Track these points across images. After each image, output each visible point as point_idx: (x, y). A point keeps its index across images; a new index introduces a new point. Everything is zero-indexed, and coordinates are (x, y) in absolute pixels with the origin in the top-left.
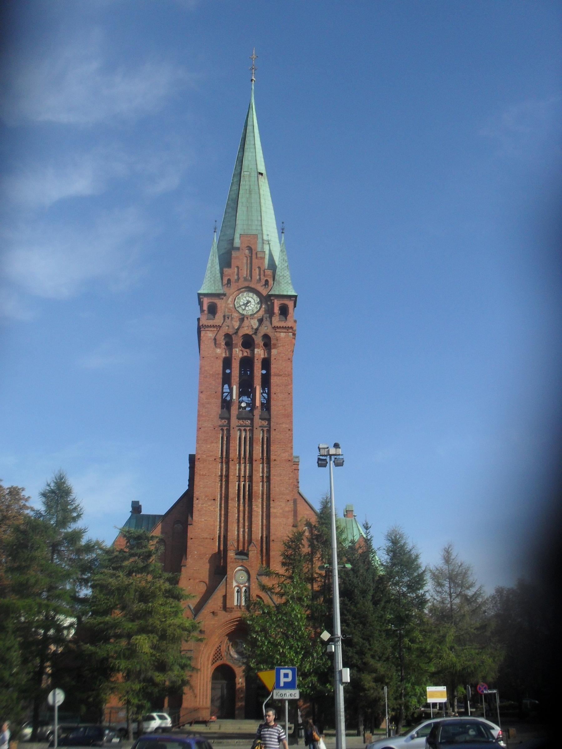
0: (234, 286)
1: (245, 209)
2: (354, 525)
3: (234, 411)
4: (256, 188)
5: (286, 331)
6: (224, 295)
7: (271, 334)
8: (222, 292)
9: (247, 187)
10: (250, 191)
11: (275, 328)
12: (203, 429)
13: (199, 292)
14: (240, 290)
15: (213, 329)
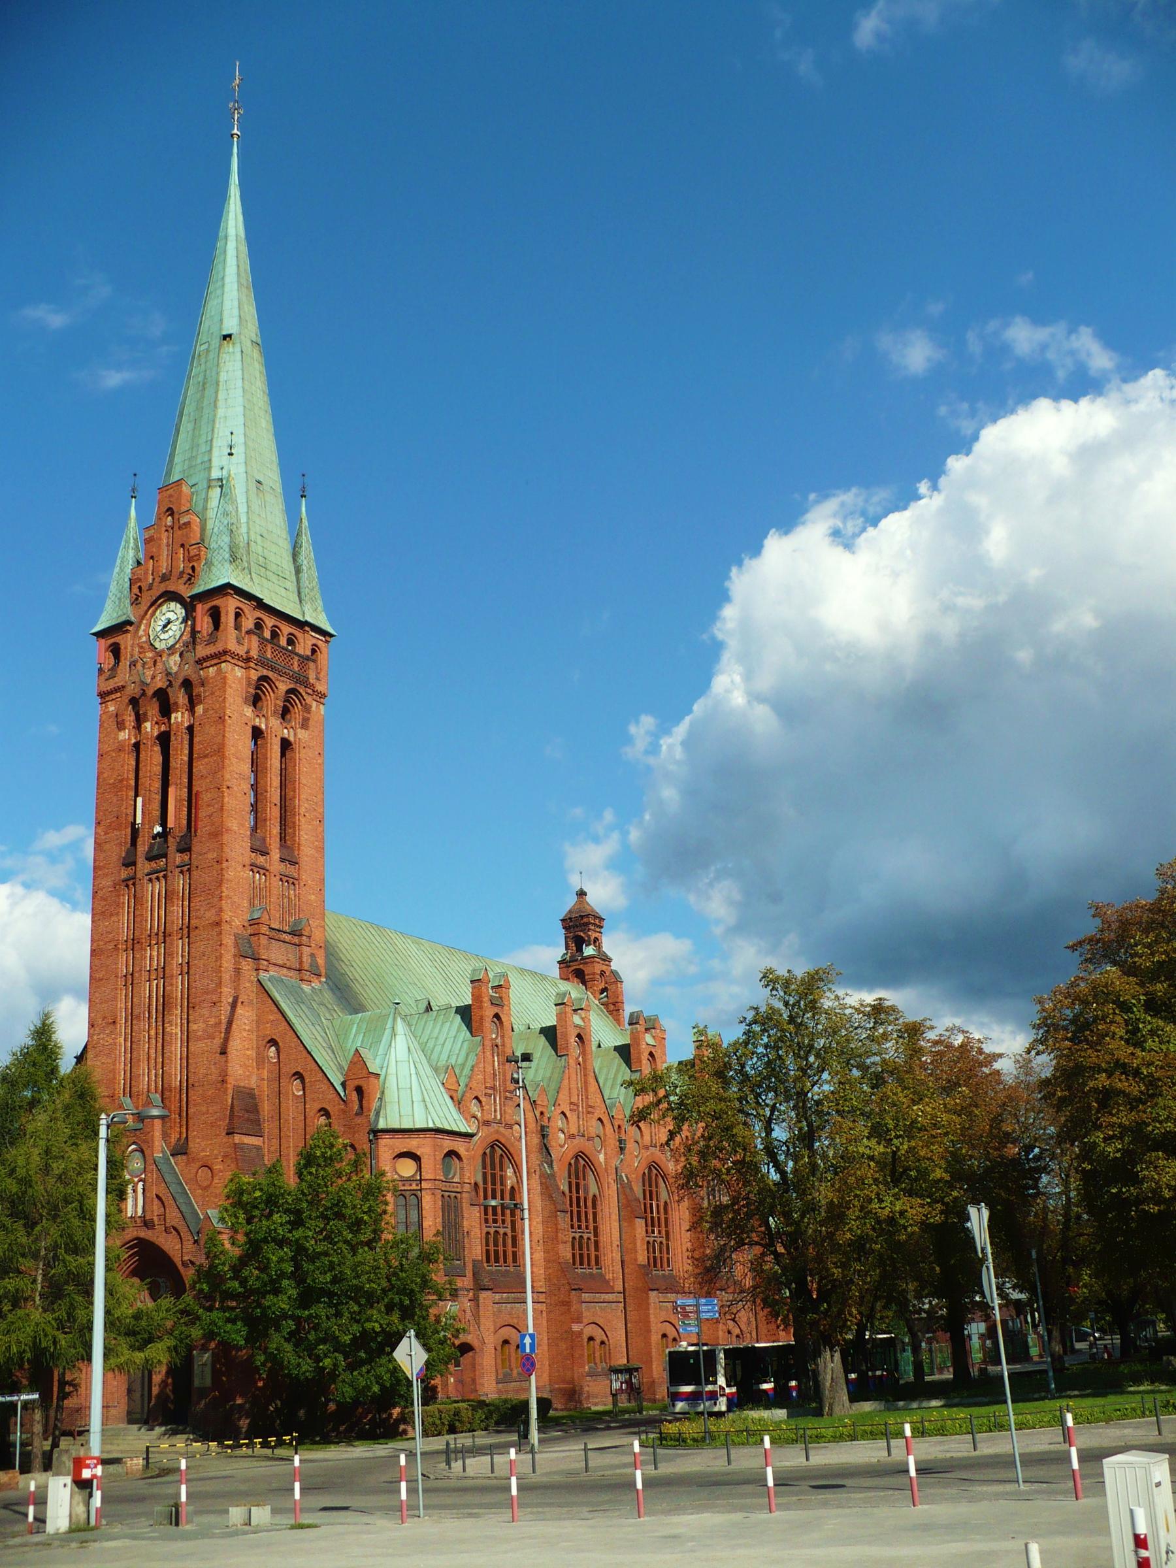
0: (146, 599)
1: (190, 426)
2: (389, 1025)
3: (142, 849)
4: (214, 373)
5: (216, 661)
6: (129, 623)
7: (194, 678)
8: (123, 618)
9: (200, 379)
10: (204, 384)
11: (200, 662)
12: (100, 894)
13: (94, 631)
14: (155, 604)
15: (114, 696)
